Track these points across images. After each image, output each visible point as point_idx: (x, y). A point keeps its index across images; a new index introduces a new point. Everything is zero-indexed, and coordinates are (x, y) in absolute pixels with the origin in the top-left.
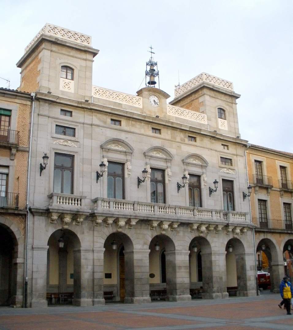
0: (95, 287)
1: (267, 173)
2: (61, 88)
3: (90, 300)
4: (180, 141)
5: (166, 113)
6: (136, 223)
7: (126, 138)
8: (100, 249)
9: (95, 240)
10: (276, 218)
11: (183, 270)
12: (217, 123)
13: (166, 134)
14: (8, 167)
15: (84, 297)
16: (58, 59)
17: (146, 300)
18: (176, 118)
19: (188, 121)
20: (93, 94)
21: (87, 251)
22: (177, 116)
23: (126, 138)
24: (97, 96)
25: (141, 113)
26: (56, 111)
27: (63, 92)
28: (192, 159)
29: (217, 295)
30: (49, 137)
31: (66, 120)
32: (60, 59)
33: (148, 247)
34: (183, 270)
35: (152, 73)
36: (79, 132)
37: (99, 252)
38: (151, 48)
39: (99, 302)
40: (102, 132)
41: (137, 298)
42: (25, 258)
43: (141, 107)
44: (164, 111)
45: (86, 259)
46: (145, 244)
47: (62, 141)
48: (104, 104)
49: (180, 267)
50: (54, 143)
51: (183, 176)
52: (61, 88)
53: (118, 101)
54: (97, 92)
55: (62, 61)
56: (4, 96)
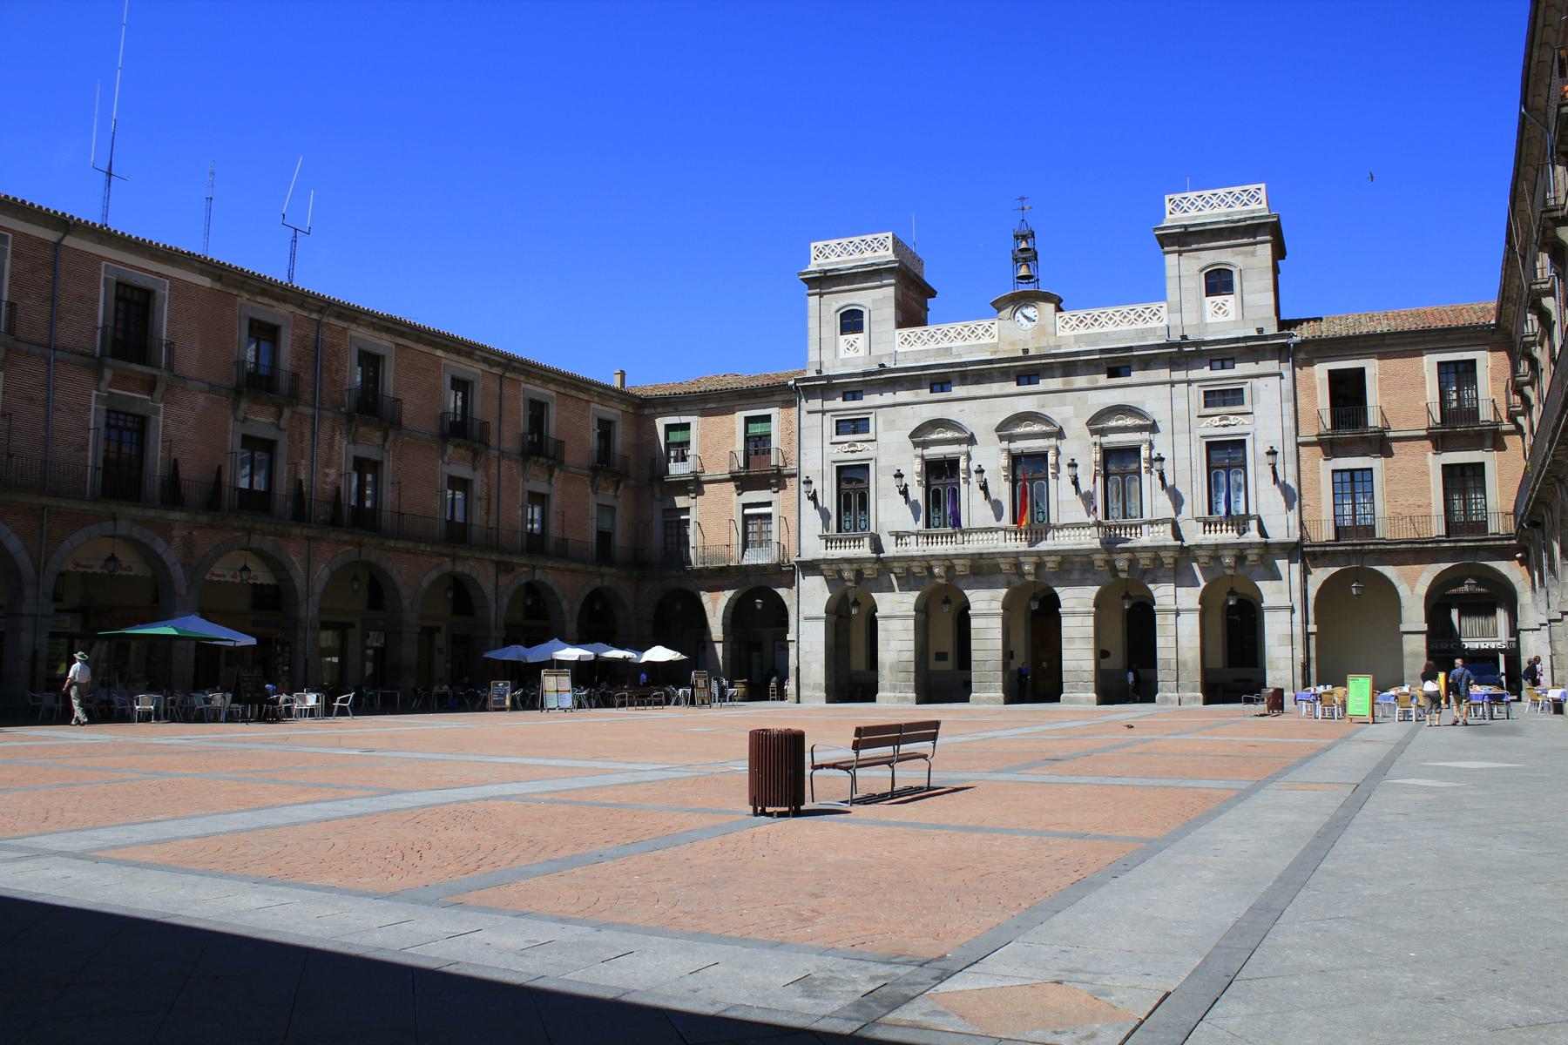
1: (1382, 395)
7: (961, 411)
10: (1406, 512)
11: (1078, 644)
12: (1201, 312)
14: (769, 504)
15: (883, 690)
16: (834, 303)
17: (995, 700)
18: (1077, 338)
20: (899, 350)
22: (1082, 331)
23: (961, 411)
24: (906, 348)
25: (992, 353)
27: (845, 362)
32: (836, 302)
33: (999, 605)
34: (1078, 644)
35: (1028, 256)
38: (1022, 199)
40: (914, 413)
41: (977, 694)
43: (996, 340)
44: (1050, 329)
45: (886, 631)
47: (846, 445)
48: (916, 361)
49: (1071, 639)
50: (835, 451)
51: (1070, 461)
52: (842, 355)
53: (945, 344)
54: (906, 339)
55: (842, 303)
56: (756, 397)
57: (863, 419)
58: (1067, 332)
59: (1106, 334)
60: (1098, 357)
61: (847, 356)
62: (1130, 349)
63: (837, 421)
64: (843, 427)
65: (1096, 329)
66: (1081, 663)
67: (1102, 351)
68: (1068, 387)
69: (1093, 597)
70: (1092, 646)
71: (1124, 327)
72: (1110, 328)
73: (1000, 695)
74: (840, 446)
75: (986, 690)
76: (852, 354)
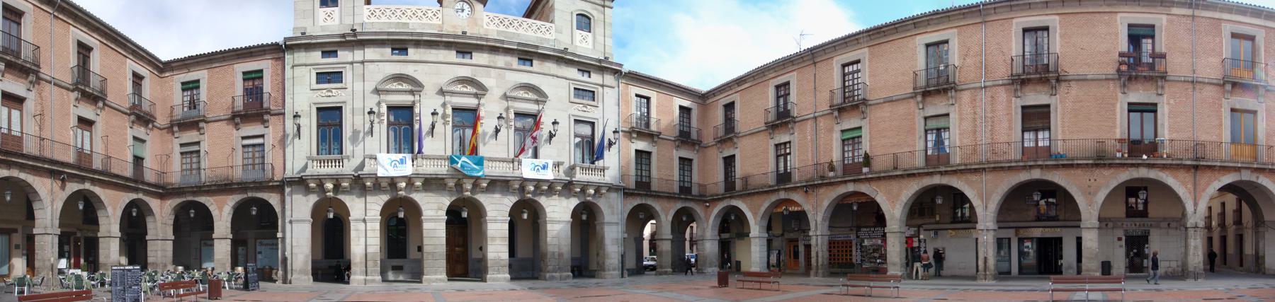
0: (369, 263)
2: (321, 23)
3: (362, 277)
4: (503, 66)
5: (483, 27)
6: (423, 184)
8: (375, 218)
9: (368, 207)
11: (498, 242)
13: (480, 58)
15: (355, 274)
18: (499, 32)
19: (519, 36)
21: (356, 220)
22: (502, 28)
26: (316, 56)
28: (521, 92)
29: (553, 276)
30: (308, 90)
31: (329, 64)
34: (498, 242)
36: (348, 76)
37: (373, 220)
39: (373, 281)
42: (284, 231)
45: (357, 230)
46: (440, 209)
47: (324, 91)
49: (494, 238)
57: (337, 72)
58: (492, 27)
59: (518, 35)
60: (516, 47)
61: (325, 24)
62: (537, 47)
63: (317, 73)
64: (324, 77)
65: (511, 30)
66: (500, 254)
67: (519, 44)
68: (492, 64)
69: (509, 211)
70: (507, 243)
71: (530, 33)
72: (521, 31)
73: (444, 276)
74: (319, 92)
75: (436, 273)
76: (329, 22)
